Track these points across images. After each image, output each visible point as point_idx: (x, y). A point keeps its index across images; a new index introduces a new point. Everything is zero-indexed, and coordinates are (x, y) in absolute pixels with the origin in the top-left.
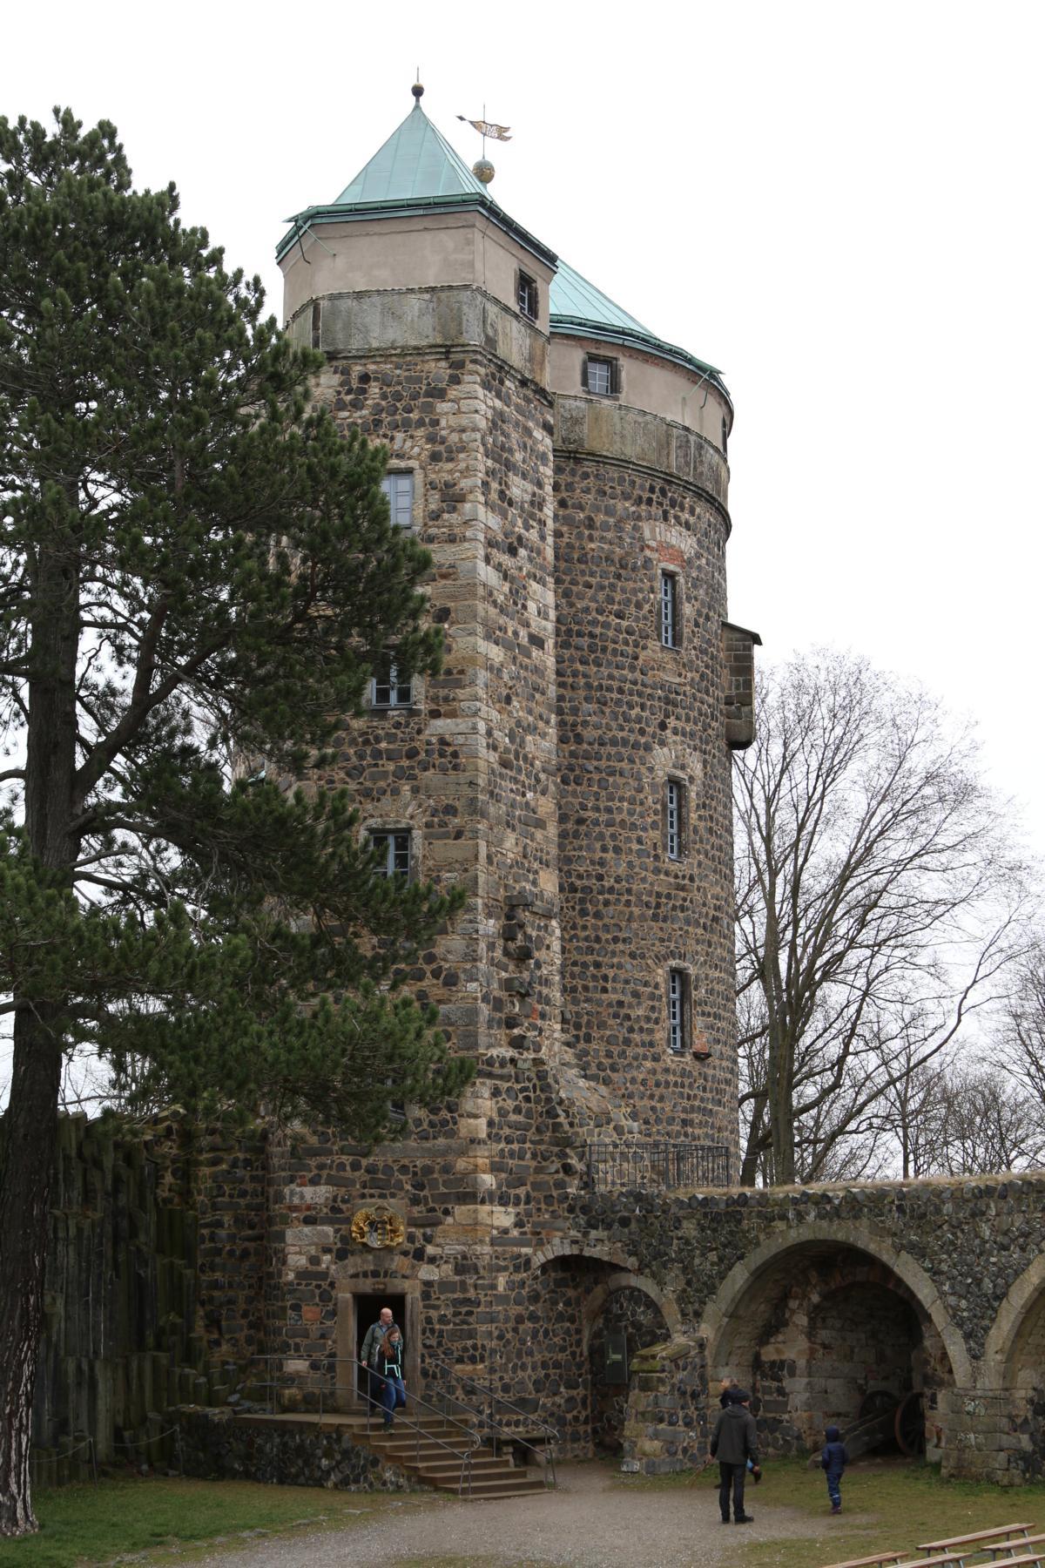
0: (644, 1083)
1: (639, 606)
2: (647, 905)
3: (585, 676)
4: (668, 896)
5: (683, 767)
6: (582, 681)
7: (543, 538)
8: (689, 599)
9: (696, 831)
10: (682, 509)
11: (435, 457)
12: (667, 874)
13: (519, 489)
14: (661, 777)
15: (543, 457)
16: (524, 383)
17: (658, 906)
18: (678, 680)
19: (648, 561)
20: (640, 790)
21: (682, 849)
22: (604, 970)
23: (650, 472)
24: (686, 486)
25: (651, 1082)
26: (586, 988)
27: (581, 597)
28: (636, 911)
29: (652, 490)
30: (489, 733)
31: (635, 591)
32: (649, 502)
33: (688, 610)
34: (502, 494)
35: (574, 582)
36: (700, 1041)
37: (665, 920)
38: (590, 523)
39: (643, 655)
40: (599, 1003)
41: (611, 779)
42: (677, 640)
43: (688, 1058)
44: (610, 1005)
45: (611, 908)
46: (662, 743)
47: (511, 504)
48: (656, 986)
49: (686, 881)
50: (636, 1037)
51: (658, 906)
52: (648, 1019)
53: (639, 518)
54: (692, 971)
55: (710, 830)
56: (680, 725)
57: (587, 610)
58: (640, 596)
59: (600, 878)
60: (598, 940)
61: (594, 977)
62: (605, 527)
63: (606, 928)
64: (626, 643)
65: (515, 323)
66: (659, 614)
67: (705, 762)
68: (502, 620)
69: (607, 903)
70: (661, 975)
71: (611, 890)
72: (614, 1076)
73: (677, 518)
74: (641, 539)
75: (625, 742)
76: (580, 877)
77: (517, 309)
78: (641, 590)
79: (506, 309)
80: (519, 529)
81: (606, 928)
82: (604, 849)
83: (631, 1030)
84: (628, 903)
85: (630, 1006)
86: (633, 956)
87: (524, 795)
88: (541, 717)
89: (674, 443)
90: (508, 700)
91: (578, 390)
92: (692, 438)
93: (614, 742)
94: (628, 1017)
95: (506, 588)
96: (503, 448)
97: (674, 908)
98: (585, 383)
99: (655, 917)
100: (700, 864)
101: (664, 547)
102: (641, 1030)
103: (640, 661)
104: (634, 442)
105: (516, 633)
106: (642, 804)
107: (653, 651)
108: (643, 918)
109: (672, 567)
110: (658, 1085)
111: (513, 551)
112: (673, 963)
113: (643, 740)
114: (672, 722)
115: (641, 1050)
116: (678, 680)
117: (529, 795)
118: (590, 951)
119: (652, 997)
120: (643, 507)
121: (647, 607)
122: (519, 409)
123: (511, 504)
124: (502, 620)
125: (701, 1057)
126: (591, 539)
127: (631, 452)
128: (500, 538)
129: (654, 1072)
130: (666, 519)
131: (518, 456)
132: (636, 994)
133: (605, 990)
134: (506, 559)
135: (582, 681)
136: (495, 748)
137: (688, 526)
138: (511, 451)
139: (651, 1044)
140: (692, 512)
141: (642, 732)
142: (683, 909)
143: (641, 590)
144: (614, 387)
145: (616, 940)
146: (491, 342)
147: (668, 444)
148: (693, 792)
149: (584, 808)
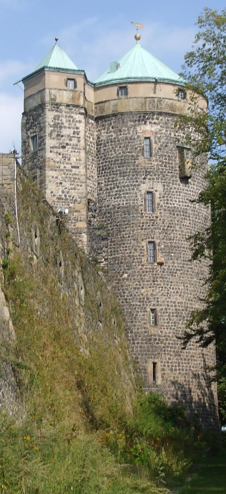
0: (139, 272)
1: (136, 149)
2: (139, 226)
3: (120, 171)
4: (147, 223)
5: (153, 188)
6: (118, 172)
7: (79, 141)
8: (156, 143)
9: (159, 204)
10: (153, 119)
11: (40, 131)
12: (146, 217)
13: (65, 132)
14: (143, 192)
15: (80, 122)
16: (68, 106)
17: (143, 226)
18: (150, 165)
19: (138, 137)
20: (137, 196)
21: (153, 210)
22: (126, 245)
23: (139, 112)
24: (153, 113)
25: (141, 271)
26: (121, 250)
27: (118, 150)
28: (136, 228)
29: (140, 117)
30: (52, 192)
31: (135, 145)
32: (139, 120)
33: (154, 146)
34: (58, 135)
35: (116, 147)
36: (160, 258)
37: (145, 229)
38: (120, 131)
39: (137, 161)
40: (124, 254)
41: (127, 196)
42: (151, 155)
43: (156, 264)
44: (127, 253)
45: (128, 229)
46: (144, 183)
47: (62, 136)
48: (143, 247)
49: (155, 218)
50: (136, 261)
51: (143, 226)
52: (140, 256)
53: (135, 126)
54: (157, 241)
55: (167, 203)
56: (151, 177)
57: (120, 153)
58: (137, 146)
59: (124, 221)
60: (124, 237)
61: (123, 247)
62: (125, 130)
63: (126, 234)
64: (132, 159)
65: (65, 92)
66: (143, 149)
67: (164, 186)
68: (57, 165)
69: (126, 228)
70: (144, 243)
71: (127, 224)
72: (129, 271)
73: (150, 123)
74: (136, 131)
75: (131, 185)
76: (119, 222)
77: (66, 88)
78: (137, 144)
79: (60, 90)
80: (67, 141)
81: (126, 234)
82: (125, 214)
83: (134, 259)
84: (133, 227)
85: (134, 253)
86: (134, 240)
87: (69, 205)
88: (78, 185)
89: (148, 103)
90: (61, 183)
91: (116, 97)
92: (156, 100)
93: (128, 186)
94: (133, 256)
95: (61, 156)
96: (58, 123)
97: (149, 226)
98: (118, 94)
99: (142, 229)
100: (161, 213)
101: (144, 132)
102: (137, 259)
103: (136, 163)
104: (133, 106)
105: (65, 167)
106: (137, 200)
107: (141, 159)
108: (138, 230)
109: (148, 136)
110: (143, 272)
111: (64, 147)
112: (148, 240)
113: (137, 184)
114: (149, 177)
115: (137, 264)
116: (150, 165)
117: (71, 205)
118: (122, 240)
119: (141, 250)
120: (137, 122)
121: (139, 148)
122: (65, 112)
123: (62, 136)
124: (57, 165)
125: (161, 264)
126: (120, 135)
127: (132, 109)
128: (57, 145)
129: (142, 269)
130: (145, 123)
131: (66, 124)
132: (136, 250)
133: (126, 250)
134: (61, 150)
135: (118, 172)
136: (54, 196)
137: (155, 123)
138: (63, 123)
139: (141, 262)
140: (158, 119)
141: (137, 181)
142: (153, 226)
143: (137, 144)
144: (126, 94)
145: (129, 237)
146: (55, 99)
147: (145, 103)
148: (157, 195)
149: (119, 204)
